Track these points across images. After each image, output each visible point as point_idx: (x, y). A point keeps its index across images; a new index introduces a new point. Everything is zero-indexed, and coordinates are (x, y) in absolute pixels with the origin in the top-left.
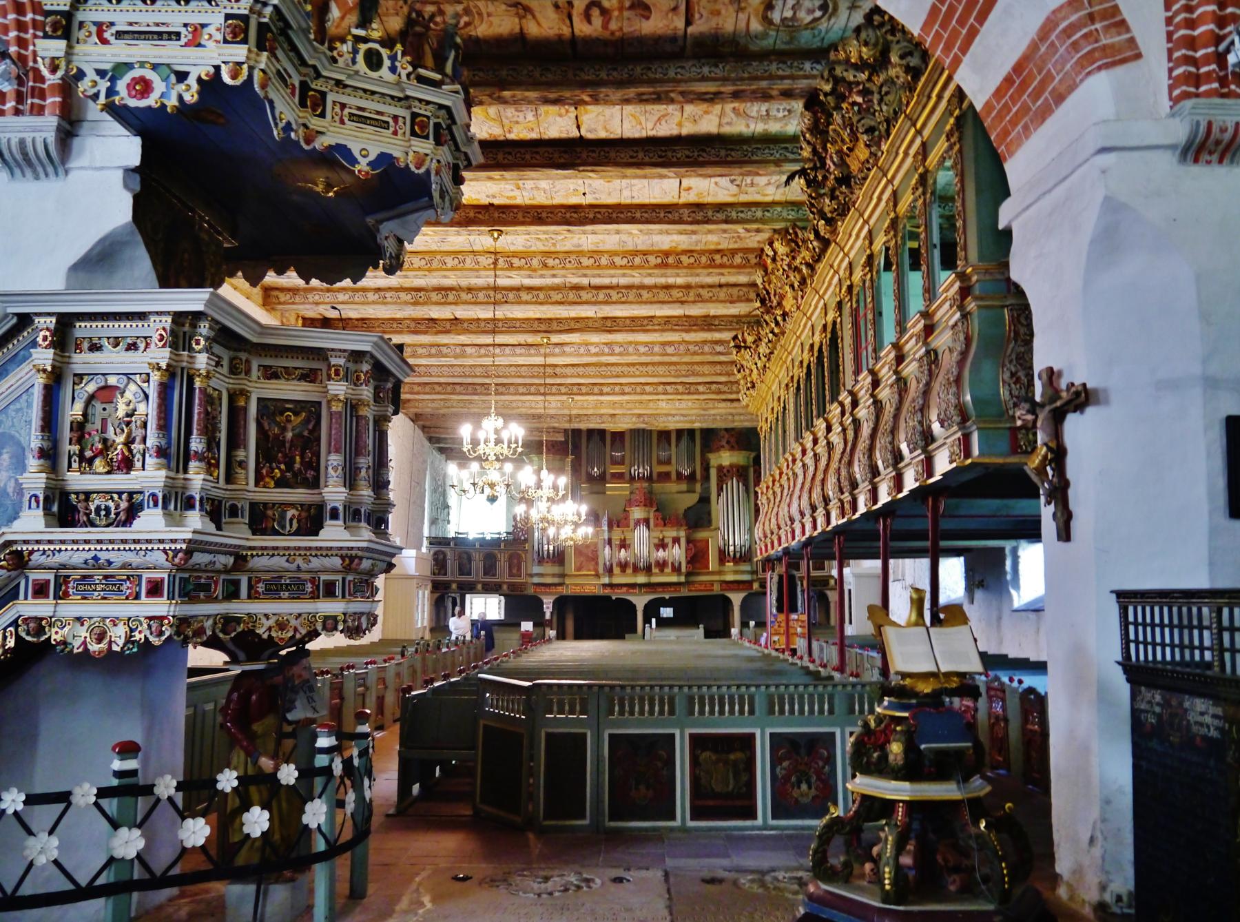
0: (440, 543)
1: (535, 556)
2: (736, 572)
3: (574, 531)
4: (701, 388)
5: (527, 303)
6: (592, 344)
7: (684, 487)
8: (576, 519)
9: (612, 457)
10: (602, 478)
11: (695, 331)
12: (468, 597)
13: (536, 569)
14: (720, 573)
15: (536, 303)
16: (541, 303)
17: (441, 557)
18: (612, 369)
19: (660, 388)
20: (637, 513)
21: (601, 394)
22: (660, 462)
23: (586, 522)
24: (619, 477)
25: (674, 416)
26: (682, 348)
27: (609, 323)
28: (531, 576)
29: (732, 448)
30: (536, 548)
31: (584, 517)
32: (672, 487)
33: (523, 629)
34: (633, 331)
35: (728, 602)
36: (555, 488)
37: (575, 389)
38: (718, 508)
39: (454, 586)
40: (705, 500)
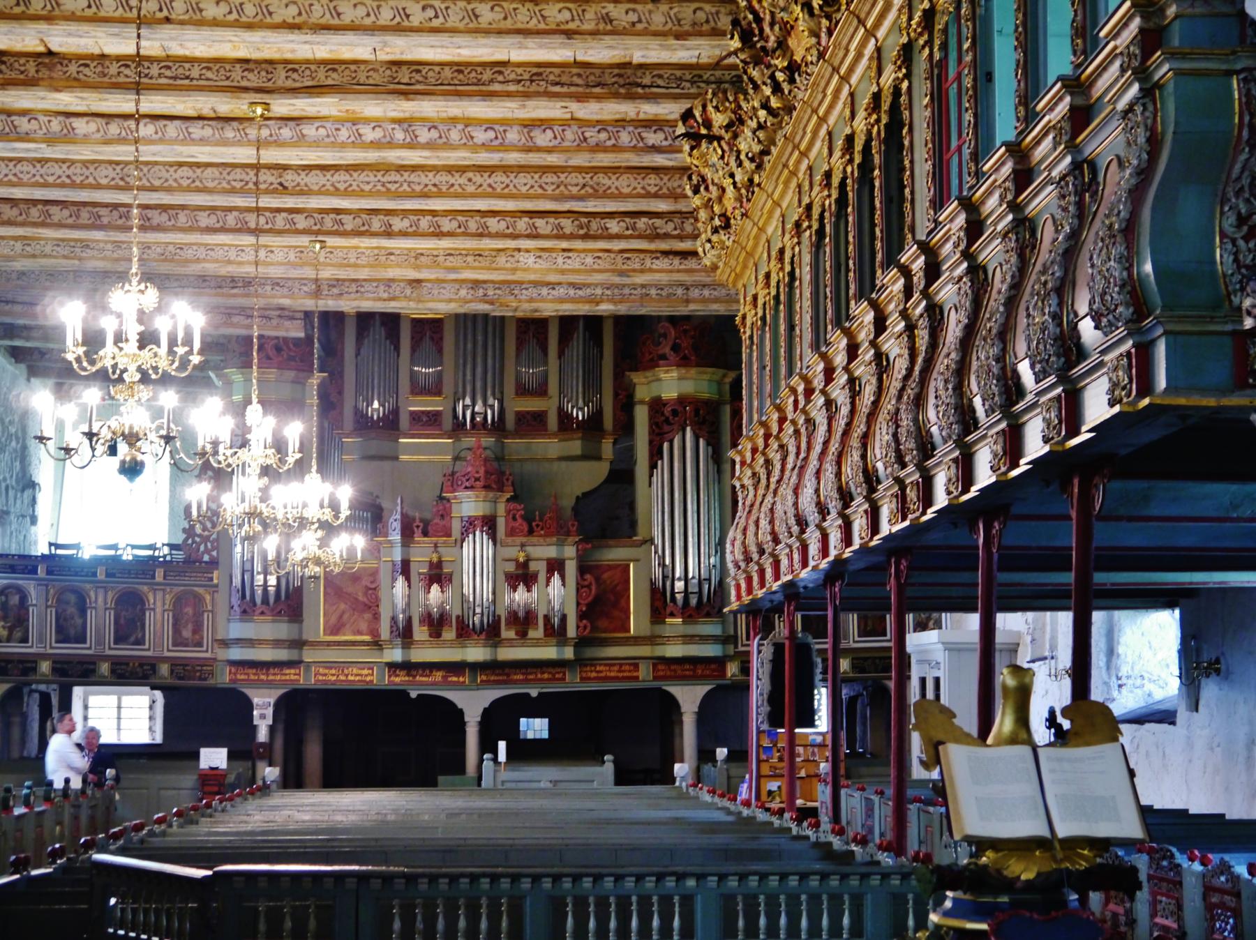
0: (12, 569)
1: (235, 601)
2: (689, 639)
3: (323, 543)
4: (614, 226)
5: (215, 23)
6: (367, 121)
7: (575, 447)
8: (327, 515)
9: (412, 373)
10: (390, 424)
11: (599, 98)
12: (78, 691)
13: (237, 630)
14: (652, 640)
15: (236, 24)
16: (249, 26)
18: (413, 177)
19: (522, 224)
20: (469, 504)
21: (388, 233)
22: (523, 390)
23: (353, 523)
24: (428, 422)
25: (552, 285)
26: (569, 135)
27: (404, 75)
28: (225, 643)
29: (684, 362)
30: (237, 581)
31: (345, 512)
32: (550, 446)
34: (459, 94)
35: (672, 705)
36: (279, 446)
37: (328, 222)
38: (652, 495)
39: (45, 667)
40: (622, 476)
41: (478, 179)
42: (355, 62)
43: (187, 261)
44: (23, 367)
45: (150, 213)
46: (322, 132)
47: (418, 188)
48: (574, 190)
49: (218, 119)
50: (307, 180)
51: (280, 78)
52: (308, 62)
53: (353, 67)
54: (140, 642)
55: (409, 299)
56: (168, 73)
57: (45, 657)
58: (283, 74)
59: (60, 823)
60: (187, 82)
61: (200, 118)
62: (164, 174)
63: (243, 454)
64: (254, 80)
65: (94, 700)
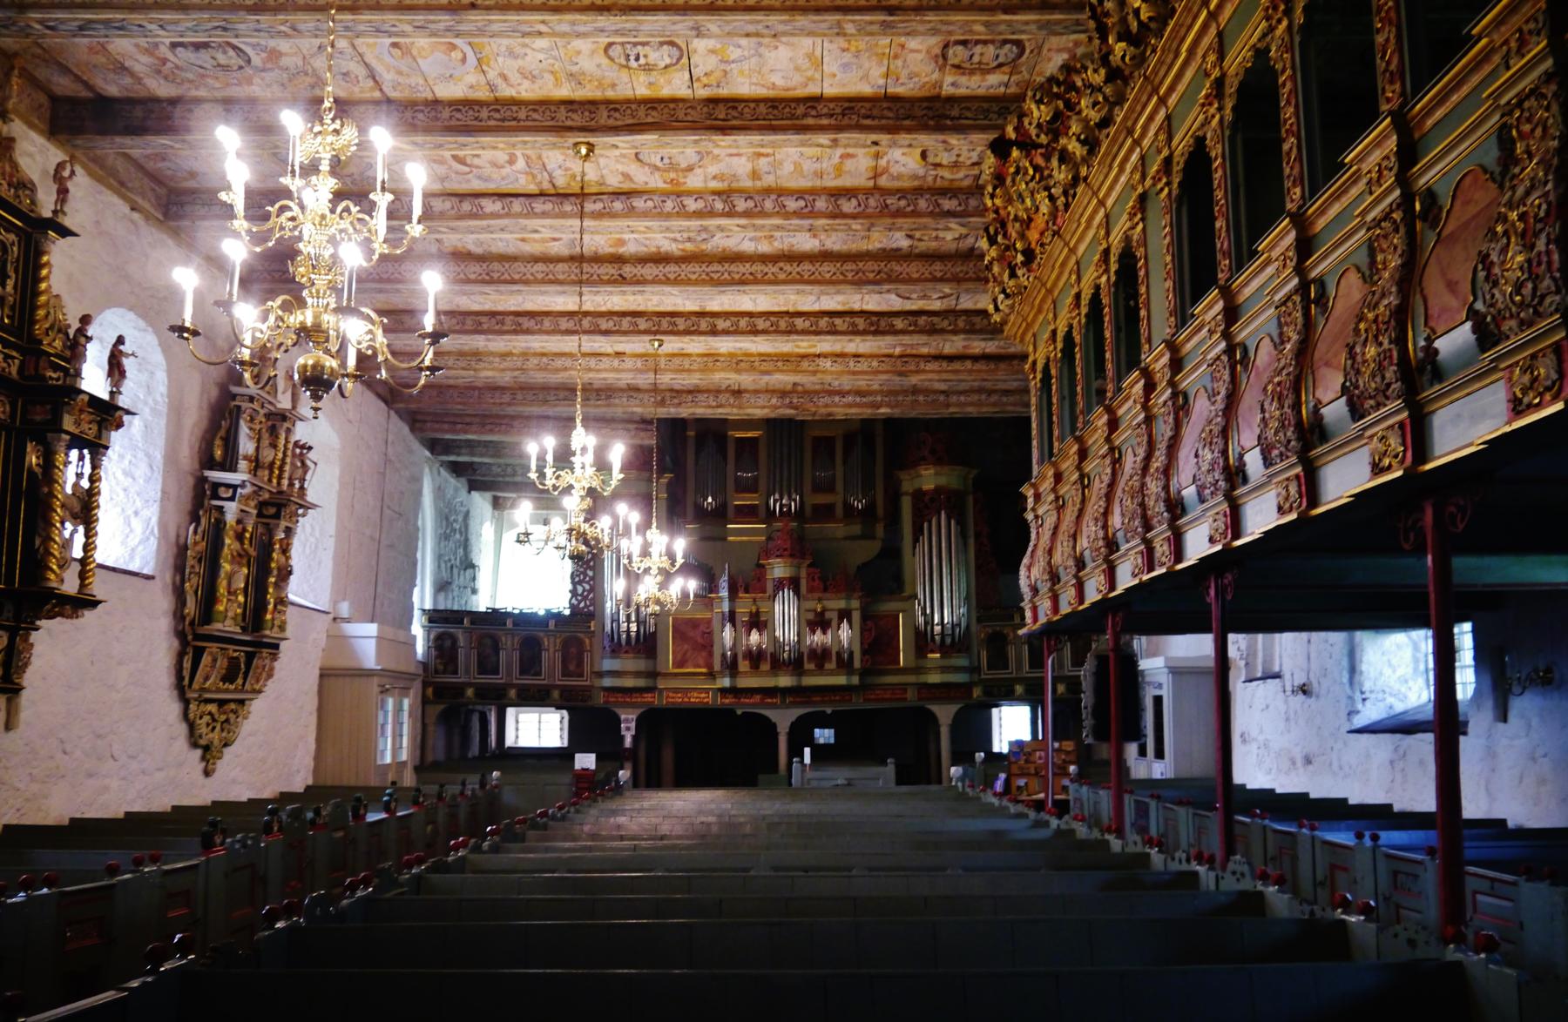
1: (607, 643)
2: (944, 669)
3: (663, 586)
6: (689, 193)
7: (856, 529)
8: (666, 564)
9: (737, 478)
10: (720, 515)
11: (909, 130)
12: (511, 711)
13: (608, 664)
14: (917, 670)
17: (448, 643)
18: (733, 268)
20: (779, 569)
21: (714, 332)
22: (818, 488)
23: (687, 569)
24: (748, 513)
25: (842, 394)
26: (872, 202)
27: (721, 112)
28: (601, 675)
29: (939, 462)
30: (608, 628)
31: (680, 561)
32: (837, 529)
33: (577, 766)
35: (933, 719)
37: (665, 323)
38: (916, 562)
39: (470, 692)
40: (891, 554)
41: (788, 268)
42: (675, 100)
43: (557, 370)
44: (463, 480)
45: (521, 320)
46: (650, 204)
47: (737, 277)
48: (871, 276)
49: (558, 195)
50: (643, 271)
51: (603, 117)
52: (628, 101)
53: (672, 106)
54: (539, 673)
55: (732, 406)
56: (497, 116)
57: (470, 685)
58: (605, 114)
59: (433, 822)
60: (514, 123)
61: (542, 194)
62: (522, 269)
63: (567, 478)
64: (577, 119)
65: (522, 717)
